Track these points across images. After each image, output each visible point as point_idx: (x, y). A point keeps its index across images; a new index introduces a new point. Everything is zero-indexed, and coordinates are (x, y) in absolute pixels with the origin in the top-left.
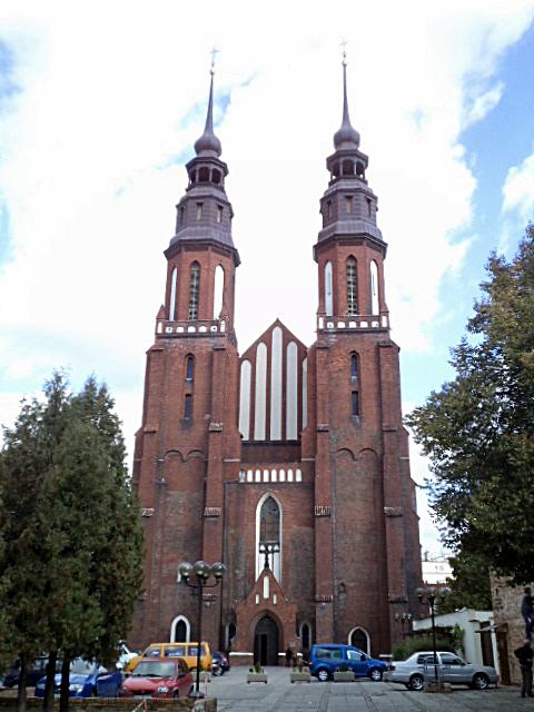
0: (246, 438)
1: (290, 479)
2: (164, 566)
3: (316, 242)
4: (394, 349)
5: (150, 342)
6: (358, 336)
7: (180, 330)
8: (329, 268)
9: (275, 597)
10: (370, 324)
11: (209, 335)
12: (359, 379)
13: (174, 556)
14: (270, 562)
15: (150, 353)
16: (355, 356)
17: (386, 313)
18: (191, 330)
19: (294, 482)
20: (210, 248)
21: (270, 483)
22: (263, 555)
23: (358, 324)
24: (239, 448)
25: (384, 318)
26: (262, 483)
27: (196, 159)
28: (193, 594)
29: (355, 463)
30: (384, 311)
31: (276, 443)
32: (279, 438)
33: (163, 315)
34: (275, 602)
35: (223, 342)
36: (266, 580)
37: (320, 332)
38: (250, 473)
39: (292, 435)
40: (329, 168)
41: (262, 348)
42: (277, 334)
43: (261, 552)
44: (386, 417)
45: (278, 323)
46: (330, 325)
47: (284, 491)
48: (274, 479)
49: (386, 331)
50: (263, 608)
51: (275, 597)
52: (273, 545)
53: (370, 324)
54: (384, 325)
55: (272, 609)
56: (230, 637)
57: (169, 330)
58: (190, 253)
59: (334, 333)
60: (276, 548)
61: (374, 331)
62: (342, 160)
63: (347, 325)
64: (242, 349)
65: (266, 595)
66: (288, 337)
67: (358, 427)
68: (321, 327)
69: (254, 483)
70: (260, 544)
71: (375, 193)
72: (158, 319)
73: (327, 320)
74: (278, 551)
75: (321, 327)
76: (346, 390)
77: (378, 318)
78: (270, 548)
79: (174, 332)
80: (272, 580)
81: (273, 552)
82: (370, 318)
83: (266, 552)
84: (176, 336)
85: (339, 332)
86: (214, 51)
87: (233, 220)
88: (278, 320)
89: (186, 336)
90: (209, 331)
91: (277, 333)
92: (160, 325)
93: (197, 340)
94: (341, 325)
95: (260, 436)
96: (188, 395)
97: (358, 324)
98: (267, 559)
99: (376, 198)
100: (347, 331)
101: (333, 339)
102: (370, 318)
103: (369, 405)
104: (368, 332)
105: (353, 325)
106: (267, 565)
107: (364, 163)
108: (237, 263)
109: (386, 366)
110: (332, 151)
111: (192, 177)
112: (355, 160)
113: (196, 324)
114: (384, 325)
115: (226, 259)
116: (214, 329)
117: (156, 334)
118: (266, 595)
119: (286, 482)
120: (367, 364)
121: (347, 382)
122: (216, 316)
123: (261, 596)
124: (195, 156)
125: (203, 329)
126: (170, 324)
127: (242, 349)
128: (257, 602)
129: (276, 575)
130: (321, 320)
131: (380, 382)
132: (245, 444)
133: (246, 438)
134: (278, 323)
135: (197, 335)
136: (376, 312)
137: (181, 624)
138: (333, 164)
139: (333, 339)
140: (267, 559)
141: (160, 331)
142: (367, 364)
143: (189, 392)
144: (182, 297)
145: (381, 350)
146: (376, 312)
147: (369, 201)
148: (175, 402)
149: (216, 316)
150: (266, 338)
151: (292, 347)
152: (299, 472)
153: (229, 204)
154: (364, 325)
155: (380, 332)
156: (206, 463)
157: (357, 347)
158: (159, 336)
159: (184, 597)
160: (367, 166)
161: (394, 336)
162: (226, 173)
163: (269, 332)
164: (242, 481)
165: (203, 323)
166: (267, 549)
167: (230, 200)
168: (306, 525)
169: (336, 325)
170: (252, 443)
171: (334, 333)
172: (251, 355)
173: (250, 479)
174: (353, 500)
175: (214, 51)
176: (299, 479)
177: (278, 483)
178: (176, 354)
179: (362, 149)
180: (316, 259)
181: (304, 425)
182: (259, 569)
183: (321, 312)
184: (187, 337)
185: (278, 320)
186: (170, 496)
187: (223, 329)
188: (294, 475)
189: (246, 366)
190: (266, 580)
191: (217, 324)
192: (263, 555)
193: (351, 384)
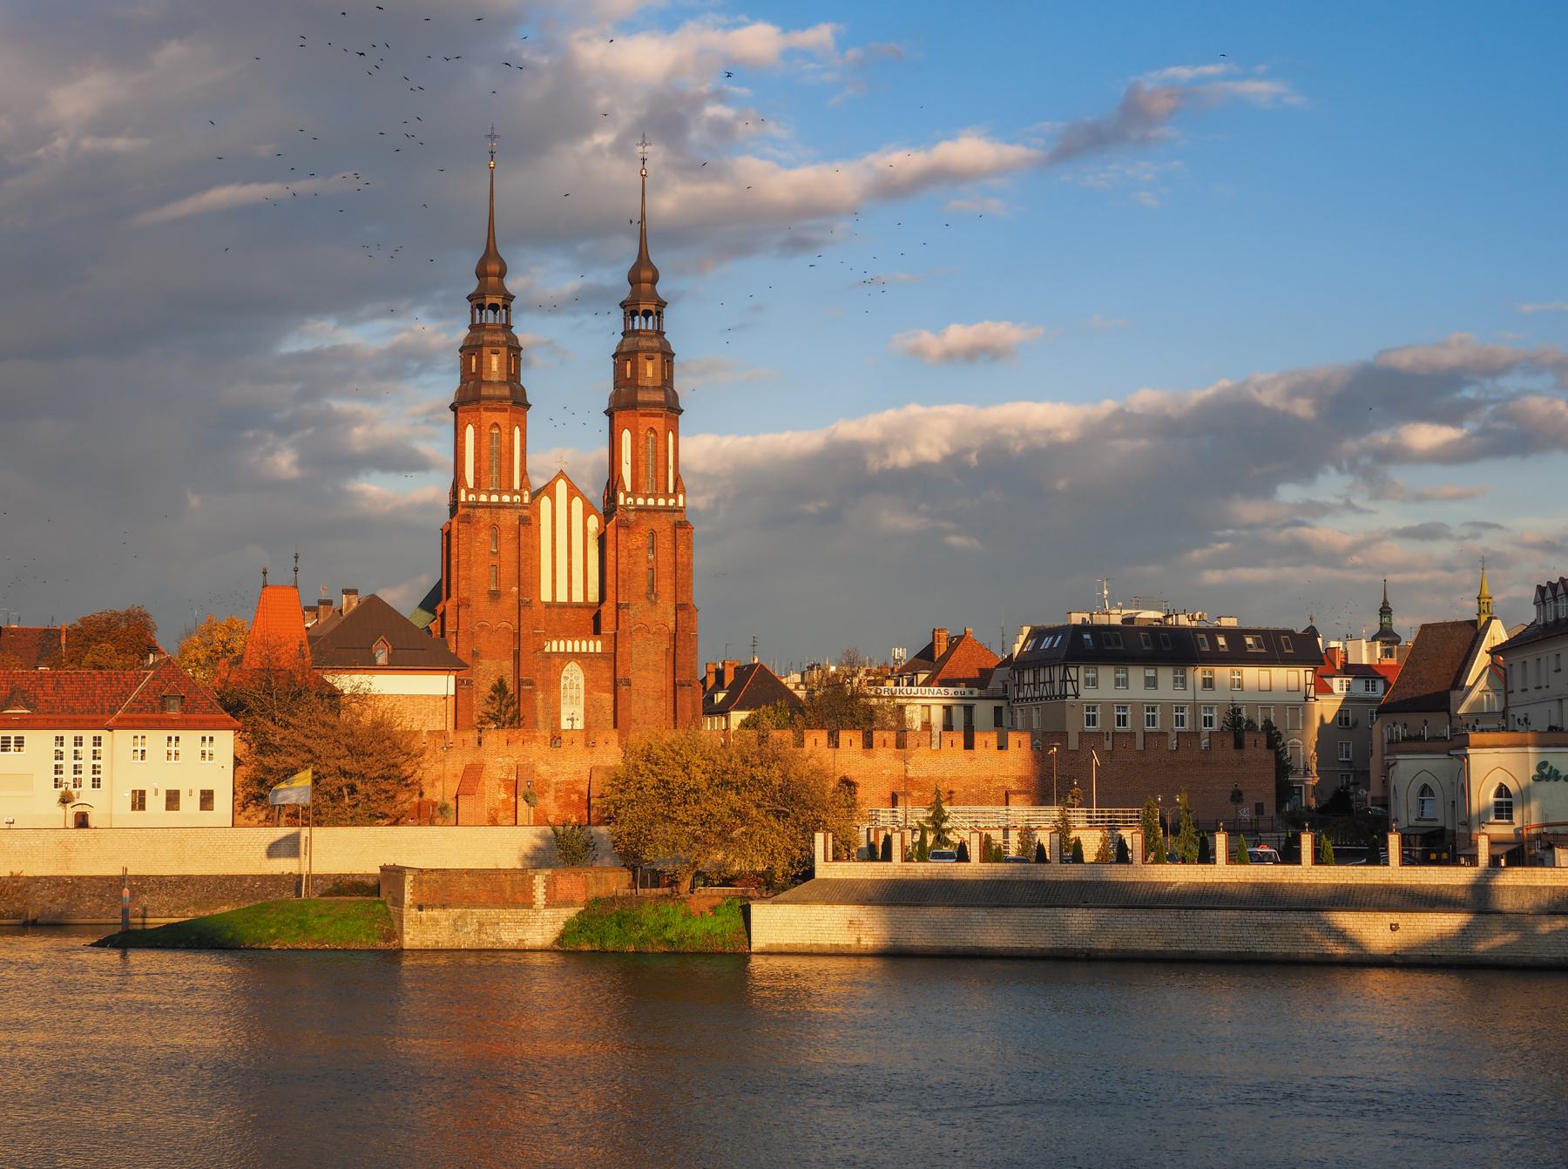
1: (591, 650)
7: (483, 498)
11: (511, 505)
12: (656, 558)
17: (684, 492)
18: (495, 498)
19: (595, 653)
21: (573, 653)
25: (681, 497)
29: (650, 636)
31: (562, 606)
41: (545, 502)
42: (561, 487)
44: (679, 595)
46: (630, 500)
47: (587, 661)
48: (577, 650)
54: (681, 504)
57: (471, 497)
58: (489, 414)
59: (633, 510)
61: (667, 509)
67: (654, 603)
76: (643, 568)
85: (639, 509)
89: (488, 506)
91: (561, 487)
93: (501, 511)
94: (640, 501)
101: (632, 517)
103: (665, 586)
105: (651, 502)
109: (681, 548)
113: (500, 493)
114: (681, 504)
116: (516, 498)
121: (644, 560)
125: (506, 498)
134: (561, 474)
135: (500, 506)
136: (671, 490)
142: (665, 544)
144: (485, 464)
146: (671, 490)
151: (577, 503)
152: (599, 643)
154: (661, 502)
155: (675, 511)
164: (547, 650)
168: (605, 691)
169: (635, 501)
173: (555, 649)
174: (646, 670)
176: (599, 650)
177: (580, 653)
184: (490, 507)
186: (481, 664)
188: (595, 646)
191: (516, 493)
193: (648, 562)
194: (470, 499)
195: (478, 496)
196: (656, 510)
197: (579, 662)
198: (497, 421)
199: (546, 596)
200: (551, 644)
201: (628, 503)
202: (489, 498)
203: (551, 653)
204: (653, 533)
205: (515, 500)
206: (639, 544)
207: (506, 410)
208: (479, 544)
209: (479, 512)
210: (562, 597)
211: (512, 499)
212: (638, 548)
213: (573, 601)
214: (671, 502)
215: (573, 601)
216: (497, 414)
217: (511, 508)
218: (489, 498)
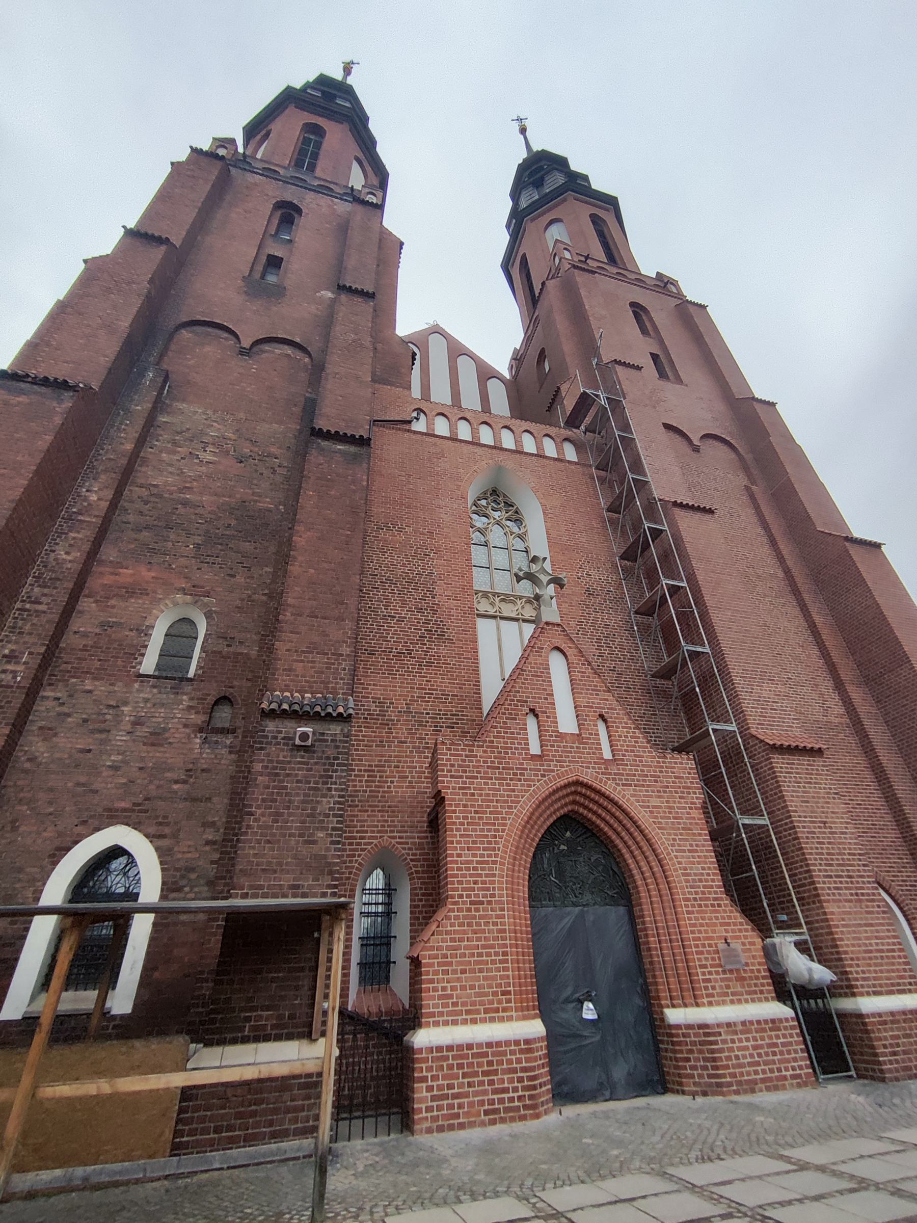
13: (147, 574)
28: (207, 729)
65: (567, 723)
118: (567, 723)
128: (535, 749)
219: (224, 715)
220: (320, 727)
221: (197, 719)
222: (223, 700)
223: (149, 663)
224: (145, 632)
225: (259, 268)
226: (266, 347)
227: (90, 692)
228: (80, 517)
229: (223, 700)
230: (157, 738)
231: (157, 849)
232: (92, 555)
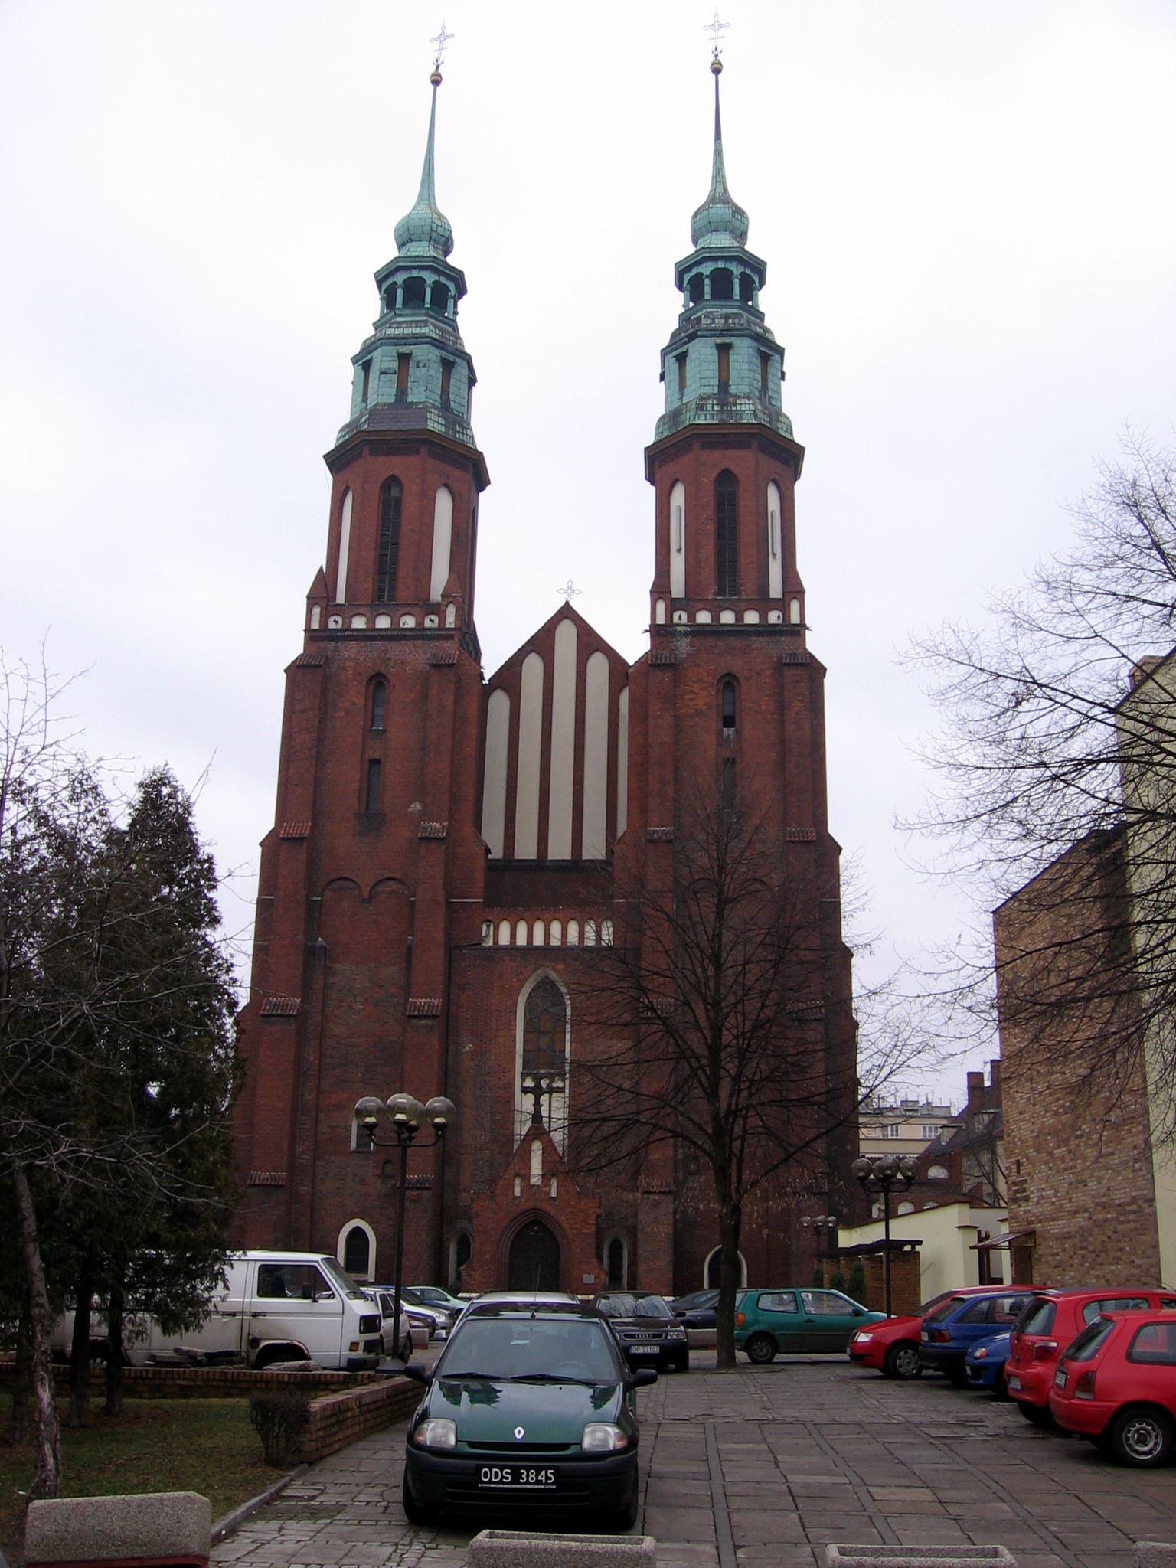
0: (497, 853)
2: (322, 1116)
3: (650, 441)
4: (814, 671)
5: (294, 647)
6: (732, 641)
7: (359, 623)
8: (678, 497)
9: (554, 1183)
10: (763, 616)
11: (419, 634)
14: (544, 1112)
15: (296, 672)
16: (729, 682)
18: (383, 622)
19: (597, 950)
20: (424, 450)
22: (530, 1099)
23: (739, 617)
24: (480, 875)
25: (795, 606)
26: (530, 948)
27: (396, 258)
30: (794, 589)
32: (566, 854)
33: (321, 593)
34: (553, 1195)
35: (451, 647)
36: (537, 1147)
37: (655, 630)
38: (505, 929)
39: (594, 848)
40: (680, 286)
41: (533, 666)
42: (566, 635)
43: (525, 1090)
45: (566, 612)
46: (680, 617)
49: (799, 630)
50: (530, 1205)
51: (554, 1183)
52: (551, 1077)
53: (763, 616)
54: (795, 619)
55: (544, 1206)
56: (459, 1263)
57: (335, 623)
58: (381, 459)
59: (686, 634)
60: (558, 1084)
62: (706, 269)
63: (716, 617)
64: (491, 664)
65: (535, 1180)
66: (590, 642)
68: (661, 620)
69: (513, 948)
70: (524, 1076)
71: (779, 340)
72: (312, 599)
73: (673, 605)
74: (561, 1090)
75: (661, 620)
77: (782, 605)
78: (544, 1083)
79: (347, 628)
80: (549, 1148)
81: (551, 1091)
82: (764, 602)
83: (537, 1092)
84: (347, 635)
86: (442, 38)
87: (475, 390)
88: (567, 603)
89: (371, 635)
90: (420, 629)
91: (566, 635)
92: (317, 611)
94: (704, 618)
95: (526, 849)
96: (374, 762)
97: (739, 617)
98: (537, 1105)
99: (780, 351)
100: (715, 631)
101: (684, 646)
102: (764, 602)
104: (758, 634)
105: (728, 618)
106: (537, 1116)
107: (756, 279)
108: (481, 480)
110: (686, 249)
111: (389, 300)
112: (736, 270)
115: (457, 473)
117: (308, 630)
118: (535, 1180)
119: (582, 949)
120: (755, 702)
122: (436, 595)
123: (526, 1177)
124: (397, 254)
126: (338, 610)
127: (491, 664)
128: (517, 1191)
129: (557, 1137)
130: (661, 606)
131: (783, 741)
132: (493, 867)
133: (497, 853)
134: (566, 612)
135: (396, 635)
137: (357, 1234)
138: (688, 277)
139: (684, 646)
140: (537, 1105)
141: (315, 626)
143: (376, 756)
145: (788, 672)
146: (776, 590)
147: (765, 359)
148: (346, 775)
149: (436, 595)
150: (542, 643)
151: (598, 666)
153: (467, 359)
154: (751, 618)
155: (782, 633)
156: (413, 904)
157: (735, 664)
158: (311, 636)
159: (363, 1182)
160: (762, 283)
161: (815, 644)
162: (462, 290)
163: (549, 630)
164: (490, 943)
165: (408, 608)
166: (538, 1085)
167: (468, 349)
169: (691, 617)
170: (509, 864)
171: (686, 634)
172: (510, 674)
173: (504, 939)
175: (442, 38)
178: (350, 674)
179: (754, 246)
180: (651, 477)
181: (622, 826)
182: (522, 1127)
183: (660, 590)
184: (373, 638)
185: (567, 603)
187: (450, 621)
189: (499, 703)
190: (537, 1147)
191: (438, 610)
192: (530, 1099)
194: (332, 625)
195: (348, 620)
196: (740, 631)
197: (561, 967)
198: (396, 472)
199: (493, 836)
200: (497, 929)
201: (676, 620)
202: (371, 621)
203: (497, 948)
204: (729, 682)
205: (428, 624)
206: (701, 702)
207: (417, 452)
208: (342, 714)
209: (350, 651)
210: (560, 849)
211: (420, 623)
212: (698, 713)
213: (586, 856)
214: (774, 617)
215: (586, 856)
216: (396, 460)
217: (414, 638)
218: (371, 621)
219: (389, 1169)
220: (419, 1192)
221: (378, 1172)
222: (387, 1162)
223: (353, 1145)
224: (348, 1129)
225: (366, 767)
226: (379, 889)
227: (333, 1162)
228: (310, 1073)
229: (387, 1162)
230: (363, 1182)
231: (372, 1228)
232: (319, 1092)
